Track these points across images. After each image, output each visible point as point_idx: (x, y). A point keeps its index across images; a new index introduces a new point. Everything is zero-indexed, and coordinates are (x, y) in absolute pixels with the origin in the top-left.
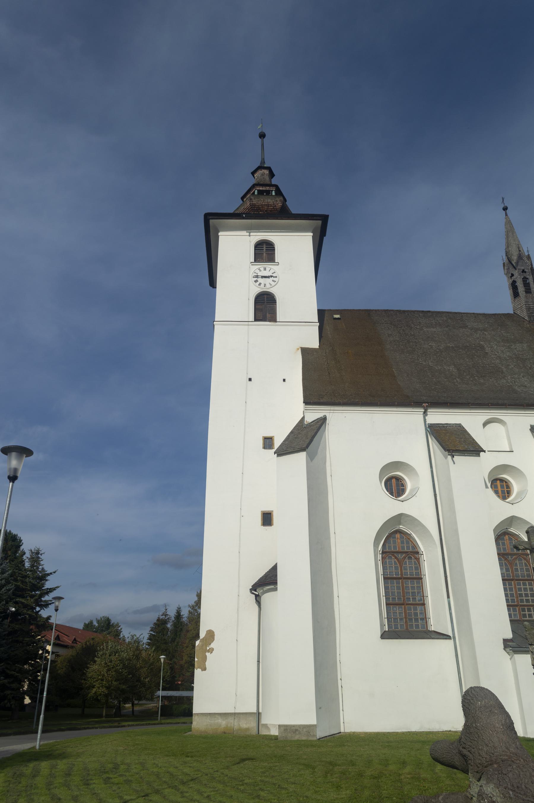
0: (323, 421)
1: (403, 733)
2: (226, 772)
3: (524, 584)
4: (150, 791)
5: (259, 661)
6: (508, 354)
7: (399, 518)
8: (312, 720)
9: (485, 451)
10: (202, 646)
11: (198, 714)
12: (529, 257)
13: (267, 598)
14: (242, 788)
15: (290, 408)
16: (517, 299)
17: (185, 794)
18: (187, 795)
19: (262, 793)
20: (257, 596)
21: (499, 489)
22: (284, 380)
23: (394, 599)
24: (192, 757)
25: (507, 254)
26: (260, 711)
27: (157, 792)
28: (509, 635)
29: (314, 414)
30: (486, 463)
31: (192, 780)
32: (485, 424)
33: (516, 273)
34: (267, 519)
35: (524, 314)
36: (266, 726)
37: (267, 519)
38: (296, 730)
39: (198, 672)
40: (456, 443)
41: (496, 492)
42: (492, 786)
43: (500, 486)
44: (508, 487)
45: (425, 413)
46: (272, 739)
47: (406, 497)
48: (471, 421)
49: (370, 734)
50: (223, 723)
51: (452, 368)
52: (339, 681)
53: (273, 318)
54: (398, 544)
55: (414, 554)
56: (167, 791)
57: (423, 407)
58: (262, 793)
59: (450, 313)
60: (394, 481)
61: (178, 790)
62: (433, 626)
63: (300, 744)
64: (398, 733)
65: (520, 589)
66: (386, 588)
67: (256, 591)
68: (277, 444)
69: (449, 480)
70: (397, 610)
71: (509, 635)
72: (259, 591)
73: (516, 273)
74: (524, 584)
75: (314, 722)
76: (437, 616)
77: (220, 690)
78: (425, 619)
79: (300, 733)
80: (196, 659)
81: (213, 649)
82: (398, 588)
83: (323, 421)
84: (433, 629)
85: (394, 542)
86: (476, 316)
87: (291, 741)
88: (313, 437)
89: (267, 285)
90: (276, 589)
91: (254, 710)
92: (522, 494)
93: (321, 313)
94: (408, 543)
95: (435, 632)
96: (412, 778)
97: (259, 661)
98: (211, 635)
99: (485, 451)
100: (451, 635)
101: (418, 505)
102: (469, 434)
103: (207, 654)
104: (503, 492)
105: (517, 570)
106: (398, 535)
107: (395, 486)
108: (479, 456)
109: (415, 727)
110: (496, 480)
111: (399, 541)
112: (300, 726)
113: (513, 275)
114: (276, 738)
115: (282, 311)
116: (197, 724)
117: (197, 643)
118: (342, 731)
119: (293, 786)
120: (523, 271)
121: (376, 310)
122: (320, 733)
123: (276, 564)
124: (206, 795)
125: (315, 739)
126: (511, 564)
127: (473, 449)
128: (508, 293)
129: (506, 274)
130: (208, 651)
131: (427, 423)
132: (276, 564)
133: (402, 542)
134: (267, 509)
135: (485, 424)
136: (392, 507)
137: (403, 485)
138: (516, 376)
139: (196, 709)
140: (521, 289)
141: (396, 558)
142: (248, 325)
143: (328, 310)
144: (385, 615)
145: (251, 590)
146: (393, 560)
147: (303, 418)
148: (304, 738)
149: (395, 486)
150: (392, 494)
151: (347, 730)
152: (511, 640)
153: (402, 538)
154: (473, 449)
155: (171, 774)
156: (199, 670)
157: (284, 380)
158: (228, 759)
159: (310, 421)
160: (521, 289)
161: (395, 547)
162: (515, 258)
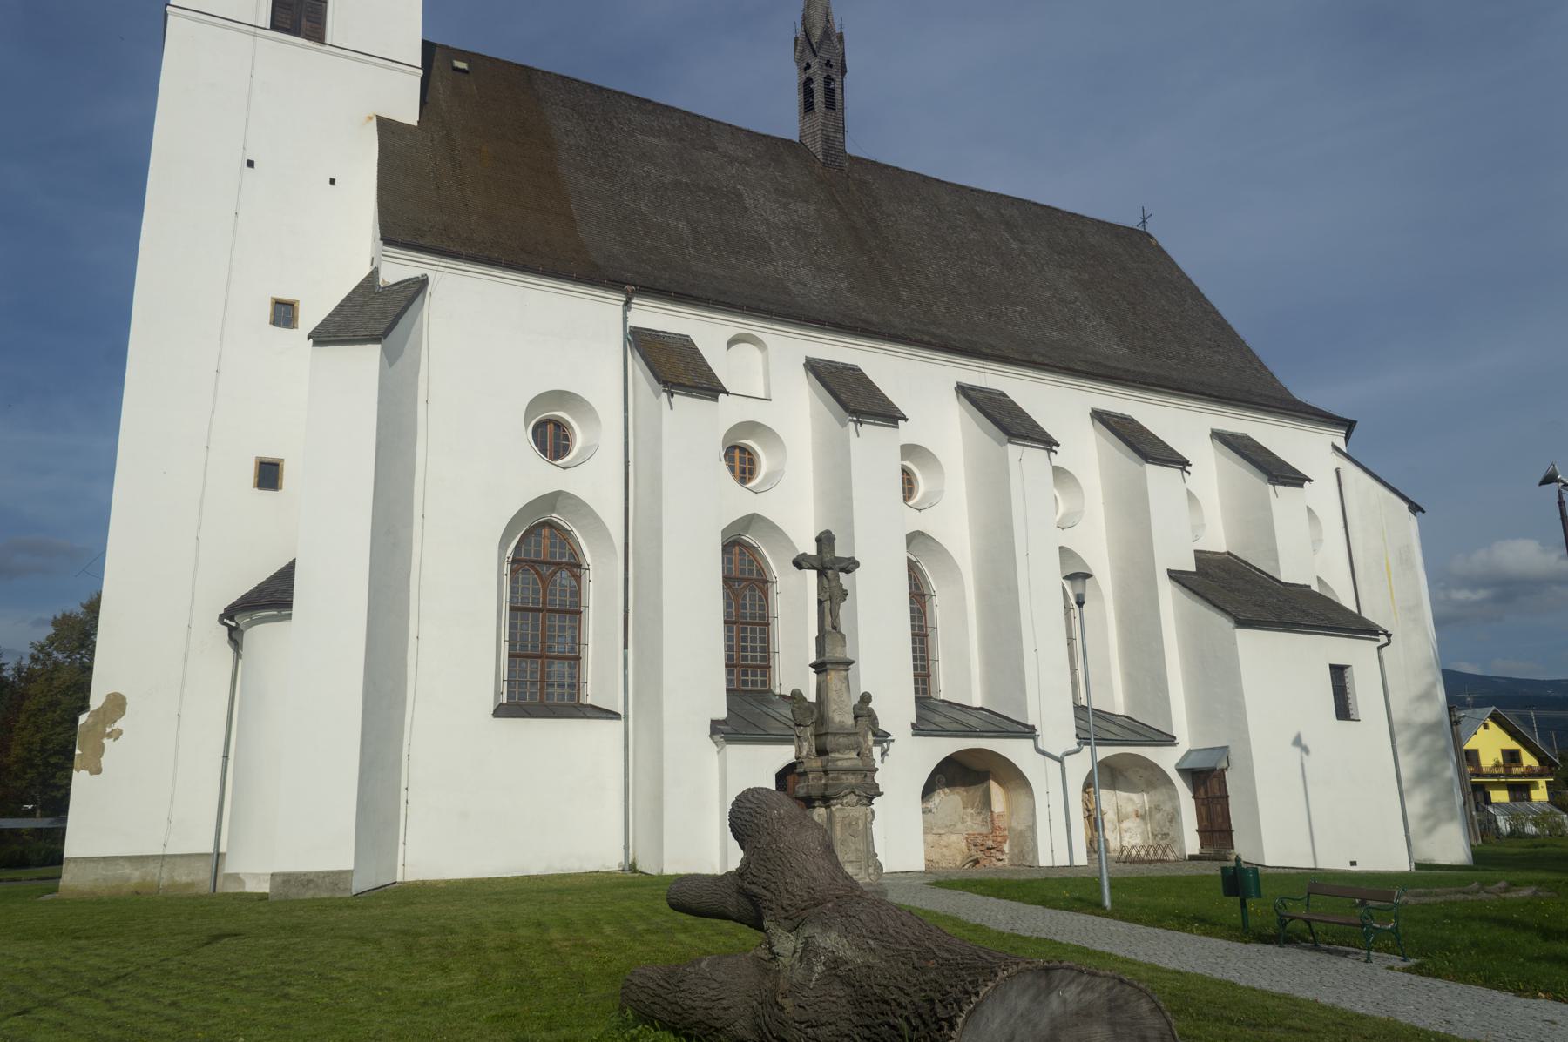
0: (418, 287)
1: (517, 878)
2: (189, 959)
3: (753, 631)
4: (28, 1004)
5: (226, 757)
6: (782, 218)
7: (554, 499)
8: (347, 863)
9: (728, 393)
10: (95, 724)
11: (75, 860)
12: (841, 37)
13: (262, 635)
14: (243, 983)
15: (344, 246)
16: (810, 116)
17: (117, 1004)
18: (123, 1004)
19: (292, 990)
20: (231, 629)
21: (737, 464)
22: (332, 182)
23: (524, 647)
24: (87, 938)
25: (805, 19)
26: (223, 849)
27: (47, 1004)
28: (722, 714)
29: (398, 268)
30: (727, 413)
31: (118, 978)
32: (731, 343)
33: (815, 64)
34: (269, 475)
35: (817, 148)
36: (236, 878)
37: (269, 475)
38: (309, 881)
39: (81, 781)
40: (677, 370)
41: (732, 469)
42: (834, 935)
43: (741, 460)
44: (752, 462)
45: (627, 305)
46: (252, 900)
47: (575, 458)
48: (708, 331)
49: (456, 881)
50: (135, 875)
51: (681, 225)
52: (403, 792)
54: (544, 547)
56: (70, 1001)
57: (626, 293)
58: (292, 990)
59: (688, 114)
60: (550, 427)
61: (97, 997)
62: (590, 696)
63: (322, 905)
64: (506, 879)
65: (744, 639)
66: (512, 626)
67: (232, 619)
68: (311, 316)
69: (658, 438)
70: (528, 666)
71: (722, 714)
72: (242, 620)
73: (815, 64)
74: (753, 631)
75: (350, 866)
76: (601, 677)
77: (126, 812)
78: (576, 685)
79: (317, 886)
80: (78, 752)
81: (120, 732)
82: (535, 627)
83: (418, 287)
84: (589, 701)
85: (538, 544)
86: (735, 131)
87: (300, 901)
88: (399, 316)
90: (289, 617)
91: (209, 848)
92: (773, 477)
93: (428, 48)
94: (562, 547)
95: (592, 706)
96: (575, 946)
97: (226, 757)
98: (117, 704)
99: (728, 393)
100: (621, 712)
101: (592, 478)
102: (702, 358)
103: (105, 741)
104: (743, 472)
105: (744, 607)
106: (546, 532)
107: (552, 438)
108: (716, 399)
109: (536, 869)
110: (734, 447)
111: (547, 542)
112: (317, 874)
113: (808, 66)
114: (263, 897)
116: (70, 878)
117: (83, 719)
118: (399, 879)
119: (351, 974)
120: (828, 64)
121: (544, 73)
122: (358, 886)
123: (291, 567)
124: (167, 1001)
125: (348, 895)
126: (736, 596)
127: (708, 387)
128: (795, 99)
129: (798, 61)
130: (109, 736)
131: (630, 323)
132: (291, 567)
133: (553, 545)
134: (270, 454)
135: (731, 343)
136: (543, 477)
137: (567, 438)
138: (792, 263)
139: (71, 849)
140: (819, 98)
141: (537, 572)
142: (255, 35)
143: (442, 47)
144: (505, 675)
145: (222, 617)
146: (532, 576)
147: (374, 274)
148: (325, 895)
149: (552, 438)
150: (543, 451)
151: (410, 878)
152: (724, 722)
153: (553, 536)
154: (708, 387)
155: (64, 971)
156: (84, 773)
157: (332, 182)
158: (180, 938)
159: (392, 281)
160: (819, 98)
161: (538, 553)
162: (817, 33)
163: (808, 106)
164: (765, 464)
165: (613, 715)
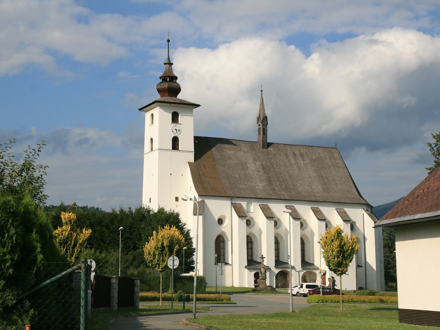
51: (237, 176)
53: (177, 149)
55: (224, 241)
78: (224, 259)
89: (177, 135)
107: (220, 221)
115: (181, 145)
160: (262, 133)
162: (262, 118)
163: (259, 134)
164: (252, 223)
165: (230, 265)
